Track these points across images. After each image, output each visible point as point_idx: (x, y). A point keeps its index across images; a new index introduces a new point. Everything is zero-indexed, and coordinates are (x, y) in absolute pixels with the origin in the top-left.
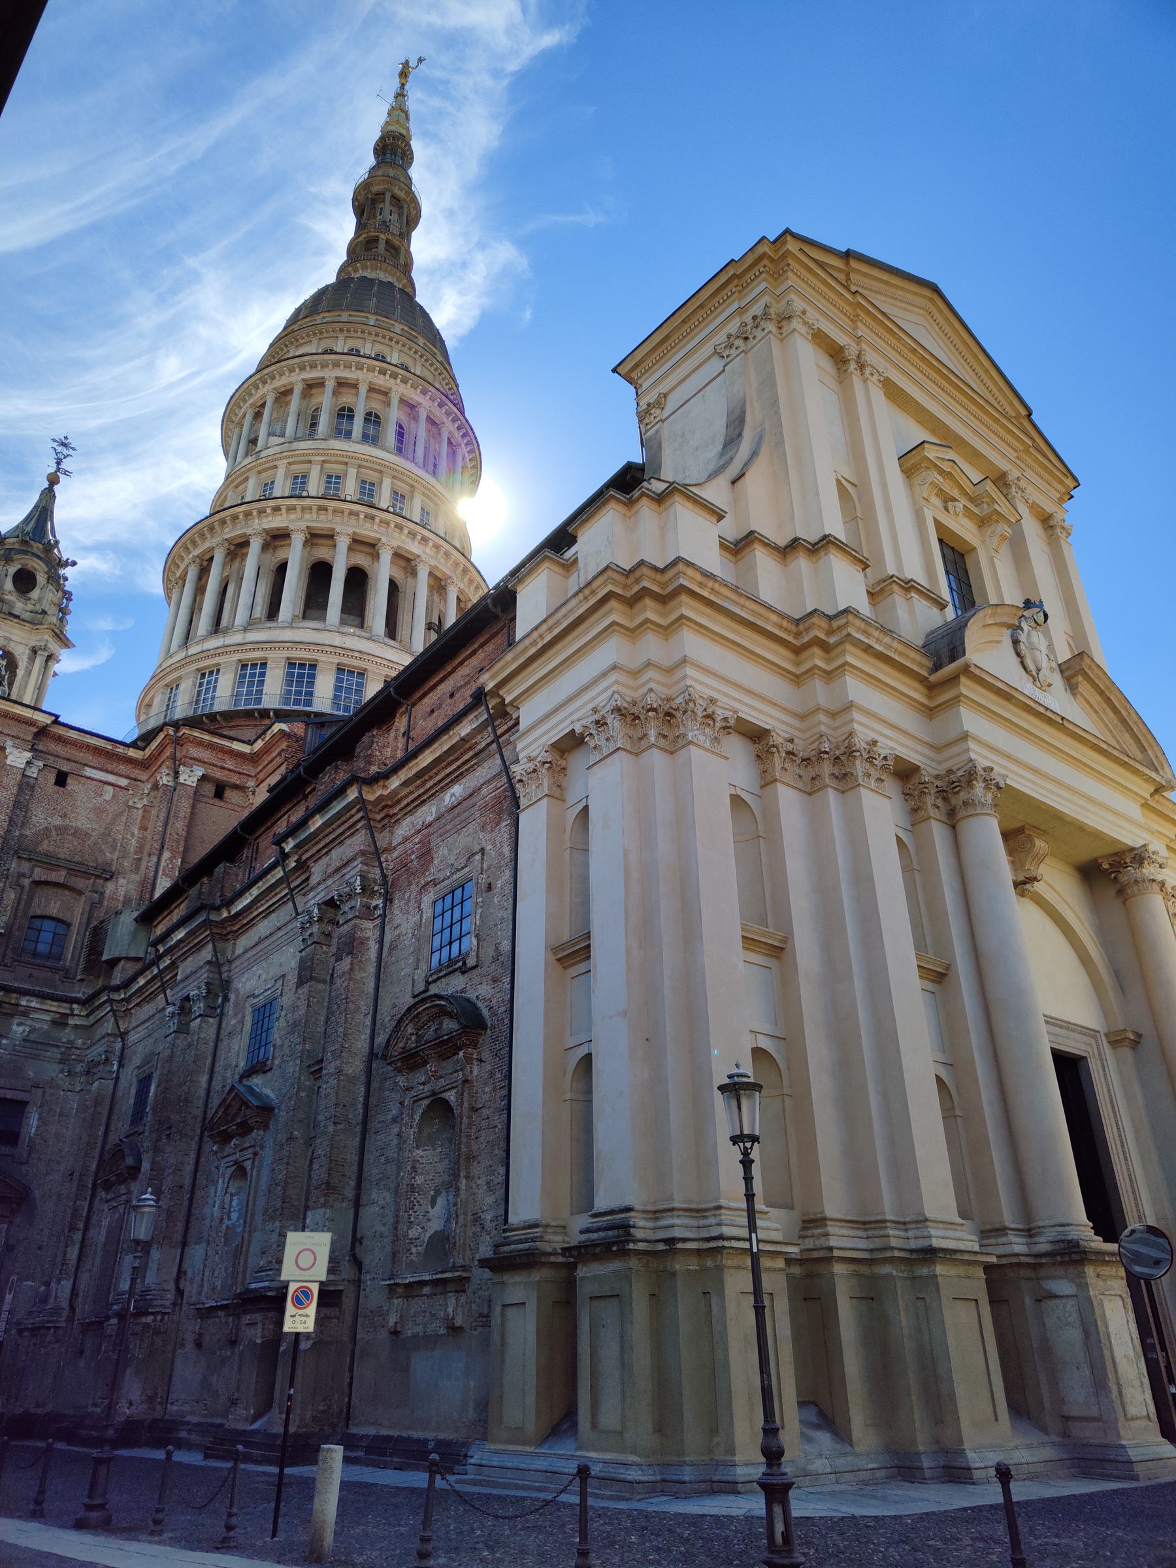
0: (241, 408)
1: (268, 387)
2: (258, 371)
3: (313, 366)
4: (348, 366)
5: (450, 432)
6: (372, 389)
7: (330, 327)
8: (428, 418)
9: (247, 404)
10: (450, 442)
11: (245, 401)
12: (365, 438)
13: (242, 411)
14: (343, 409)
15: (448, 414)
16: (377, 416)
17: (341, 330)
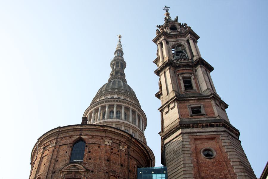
0: (87, 114)
1: (93, 109)
2: (90, 106)
3: (103, 102)
4: (111, 101)
5: (138, 113)
6: (118, 106)
7: (107, 93)
8: (132, 110)
9: (88, 113)
10: (138, 115)
11: (88, 113)
12: (117, 117)
13: (87, 115)
14: (111, 111)
15: (137, 109)
16: (119, 112)
17: (110, 93)
